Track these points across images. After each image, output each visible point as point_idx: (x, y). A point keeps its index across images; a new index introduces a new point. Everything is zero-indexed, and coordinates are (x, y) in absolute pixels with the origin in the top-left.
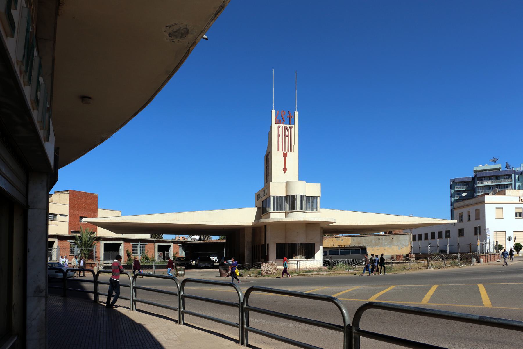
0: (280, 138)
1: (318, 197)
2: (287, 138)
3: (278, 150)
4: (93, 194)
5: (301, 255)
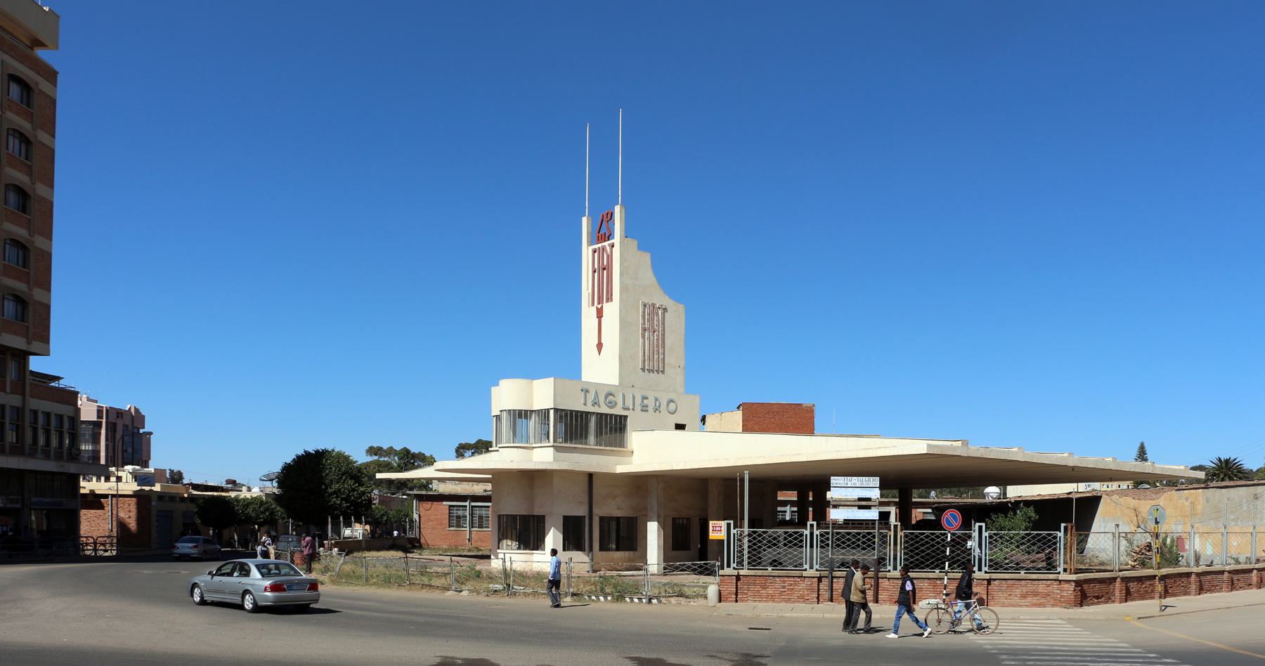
0: (596, 274)
2: (605, 271)
3: (593, 304)
4: (801, 404)
5: (507, 538)
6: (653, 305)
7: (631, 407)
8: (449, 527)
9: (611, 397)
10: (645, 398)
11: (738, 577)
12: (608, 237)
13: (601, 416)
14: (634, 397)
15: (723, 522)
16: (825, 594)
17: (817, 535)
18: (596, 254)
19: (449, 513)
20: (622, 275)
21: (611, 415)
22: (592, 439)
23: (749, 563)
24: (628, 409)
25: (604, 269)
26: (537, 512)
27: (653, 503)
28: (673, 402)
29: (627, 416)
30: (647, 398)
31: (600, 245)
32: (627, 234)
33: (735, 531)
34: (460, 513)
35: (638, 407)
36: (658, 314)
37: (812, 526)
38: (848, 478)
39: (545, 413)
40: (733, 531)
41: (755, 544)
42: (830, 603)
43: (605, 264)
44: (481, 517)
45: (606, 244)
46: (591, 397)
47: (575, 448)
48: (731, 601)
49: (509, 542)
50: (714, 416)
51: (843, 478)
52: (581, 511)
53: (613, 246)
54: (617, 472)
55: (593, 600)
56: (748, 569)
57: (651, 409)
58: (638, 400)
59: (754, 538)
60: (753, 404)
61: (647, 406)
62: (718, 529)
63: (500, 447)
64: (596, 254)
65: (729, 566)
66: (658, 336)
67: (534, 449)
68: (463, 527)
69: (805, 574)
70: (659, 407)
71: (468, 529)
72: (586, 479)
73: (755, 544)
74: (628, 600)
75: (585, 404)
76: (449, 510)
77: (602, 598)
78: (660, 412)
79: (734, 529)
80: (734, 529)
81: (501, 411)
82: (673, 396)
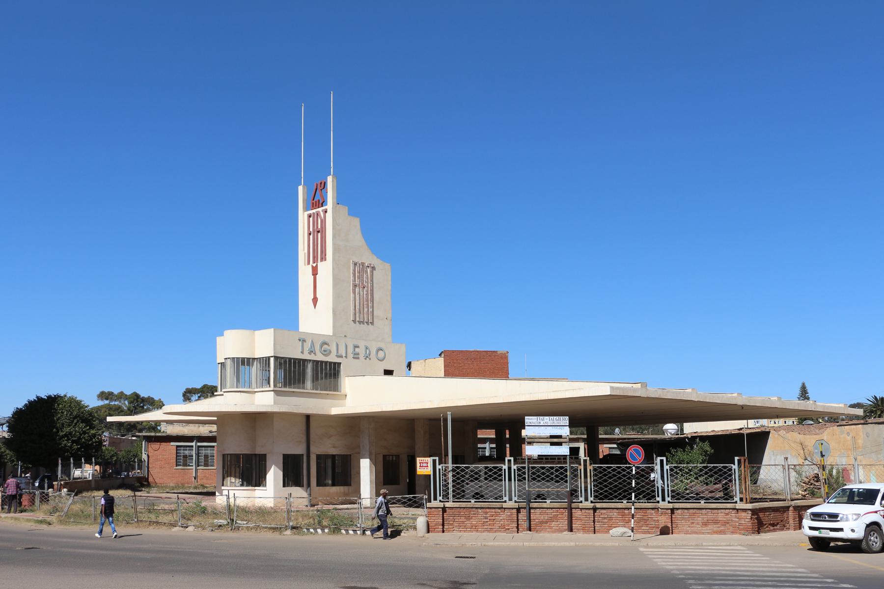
0: (311, 236)
1: (271, 357)
2: (319, 234)
3: (309, 263)
6: (363, 264)
7: (344, 355)
8: (176, 466)
9: (325, 346)
10: (356, 347)
11: (444, 509)
12: (322, 204)
13: (316, 363)
14: (346, 346)
15: (429, 459)
16: (524, 524)
17: (515, 470)
18: (311, 219)
19: (177, 453)
20: (334, 237)
21: (326, 362)
22: (309, 383)
23: (454, 496)
24: (341, 357)
25: (318, 232)
26: (259, 451)
27: (365, 442)
29: (341, 363)
30: (358, 347)
31: (314, 211)
32: (338, 202)
33: (440, 467)
34: (187, 452)
35: (351, 356)
36: (367, 272)
37: (509, 461)
38: (541, 417)
39: (266, 361)
40: (438, 467)
41: (458, 479)
42: (529, 532)
43: (319, 227)
44: (206, 457)
45: (320, 209)
47: (294, 392)
48: (438, 532)
49: (233, 480)
50: (418, 362)
51: (536, 417)
52: (300, 450)
53: (326, 212)
54: (332, 414)
55: (312, 533)
56: (453, 502)
57: (362, 356)
58: (350, 349)
59: (458, 473)
60: (453, 352)
61: (358, 354)
62: (425, 465)
63: (224, 392)
64: (311, 219)
65: (435, 499)
66: (367, 291)
67: (256, 393)
68: (189, 466)
69: (505, 505)
70: (370, 355)
71: (194, 467)
72: (304, 420)
73: (458, 479)
74: (343, 532)
75: (302, 352)
76: (177, 450)
77: (319, 531)
78: (370, 359)
79: (439, 465)
80: (439, 465)
81: (226, 359)
82: (382, 345)
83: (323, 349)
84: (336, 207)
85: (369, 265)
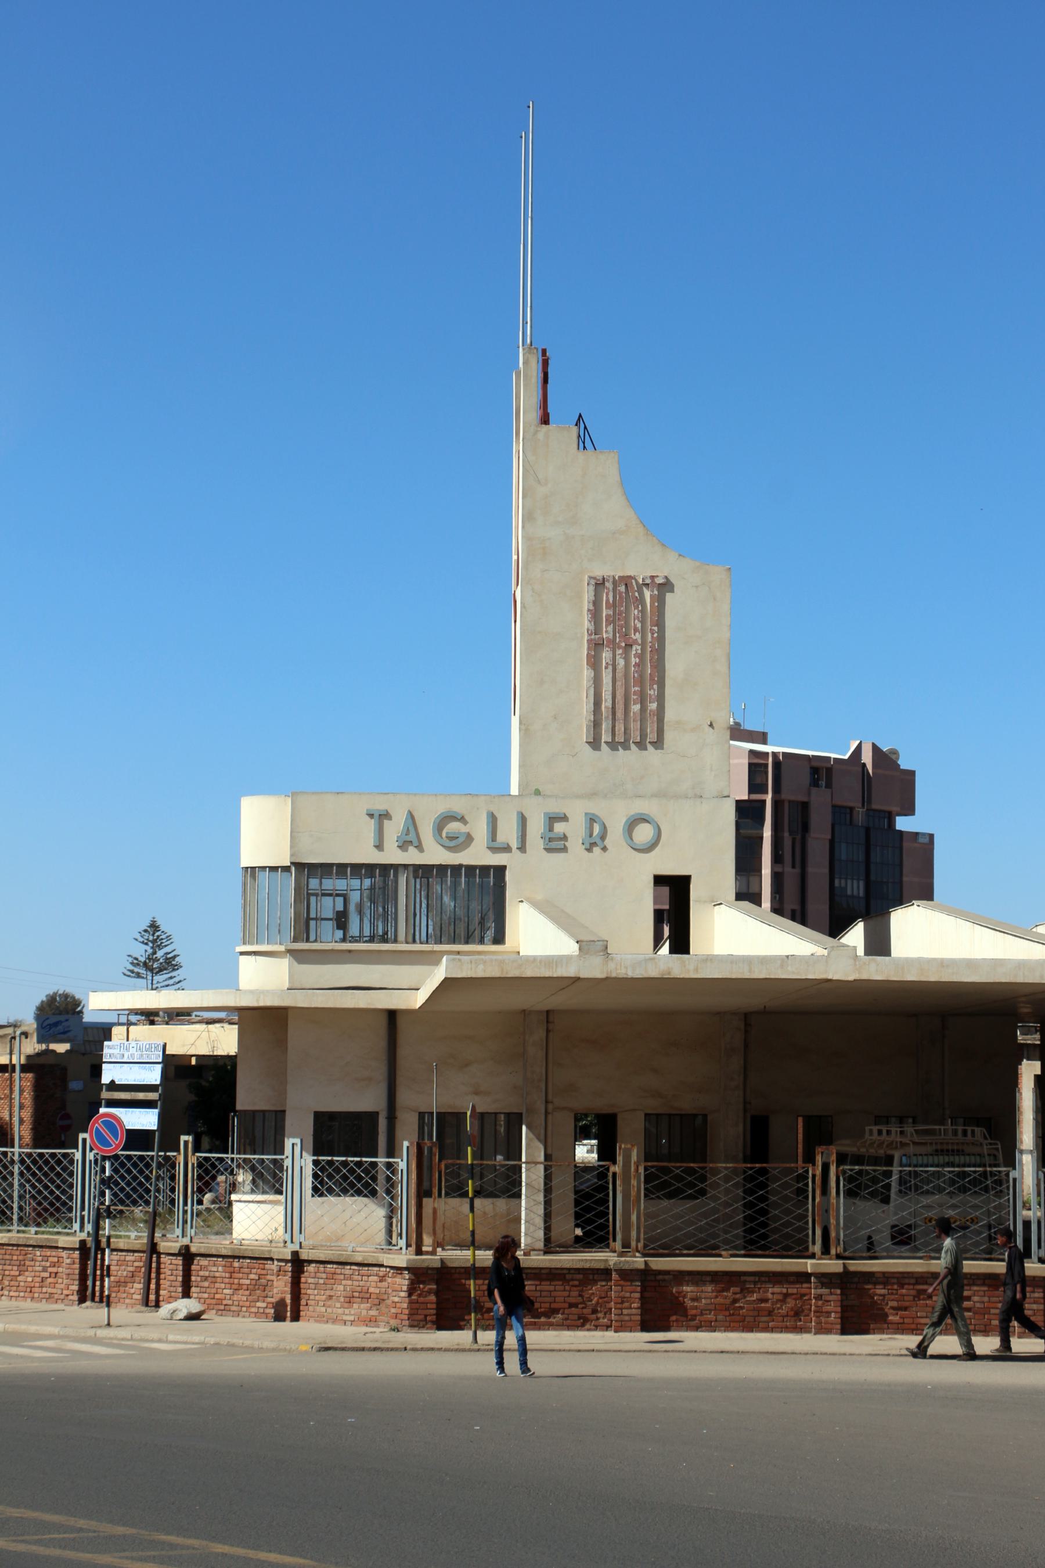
6: (627, 581)
7: (514, 844)
9: (454, 827)
10: (553, 819)
14: (523, 821)
24: (507, 849)
28: (645, 820)
29: (504, 868)
30: (564, 818)
36: (641, 600)
46: (393, 830)
57: (575, 845)
58: (536, 827)
61: (565, 838)
70: (603, 837)
75: (379, 847)
78: (604, 849)
83: (444, 835)
84: (536, 433)
85: (648, 581)
